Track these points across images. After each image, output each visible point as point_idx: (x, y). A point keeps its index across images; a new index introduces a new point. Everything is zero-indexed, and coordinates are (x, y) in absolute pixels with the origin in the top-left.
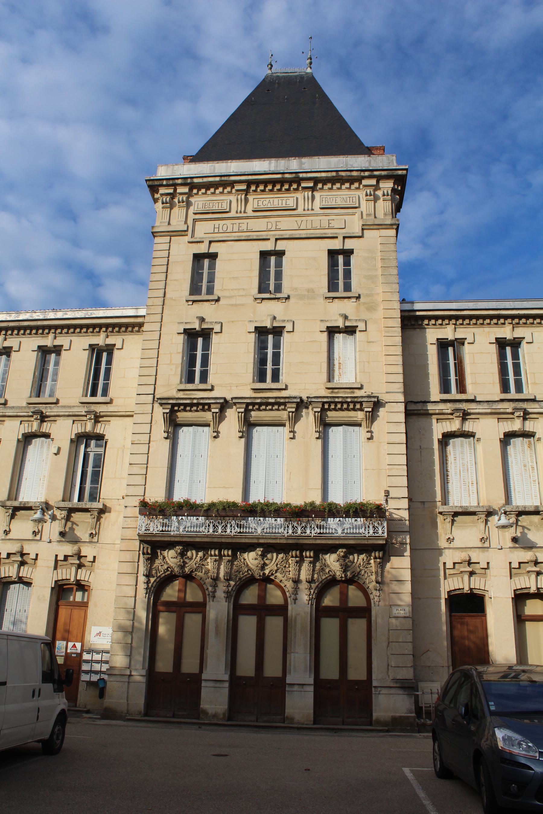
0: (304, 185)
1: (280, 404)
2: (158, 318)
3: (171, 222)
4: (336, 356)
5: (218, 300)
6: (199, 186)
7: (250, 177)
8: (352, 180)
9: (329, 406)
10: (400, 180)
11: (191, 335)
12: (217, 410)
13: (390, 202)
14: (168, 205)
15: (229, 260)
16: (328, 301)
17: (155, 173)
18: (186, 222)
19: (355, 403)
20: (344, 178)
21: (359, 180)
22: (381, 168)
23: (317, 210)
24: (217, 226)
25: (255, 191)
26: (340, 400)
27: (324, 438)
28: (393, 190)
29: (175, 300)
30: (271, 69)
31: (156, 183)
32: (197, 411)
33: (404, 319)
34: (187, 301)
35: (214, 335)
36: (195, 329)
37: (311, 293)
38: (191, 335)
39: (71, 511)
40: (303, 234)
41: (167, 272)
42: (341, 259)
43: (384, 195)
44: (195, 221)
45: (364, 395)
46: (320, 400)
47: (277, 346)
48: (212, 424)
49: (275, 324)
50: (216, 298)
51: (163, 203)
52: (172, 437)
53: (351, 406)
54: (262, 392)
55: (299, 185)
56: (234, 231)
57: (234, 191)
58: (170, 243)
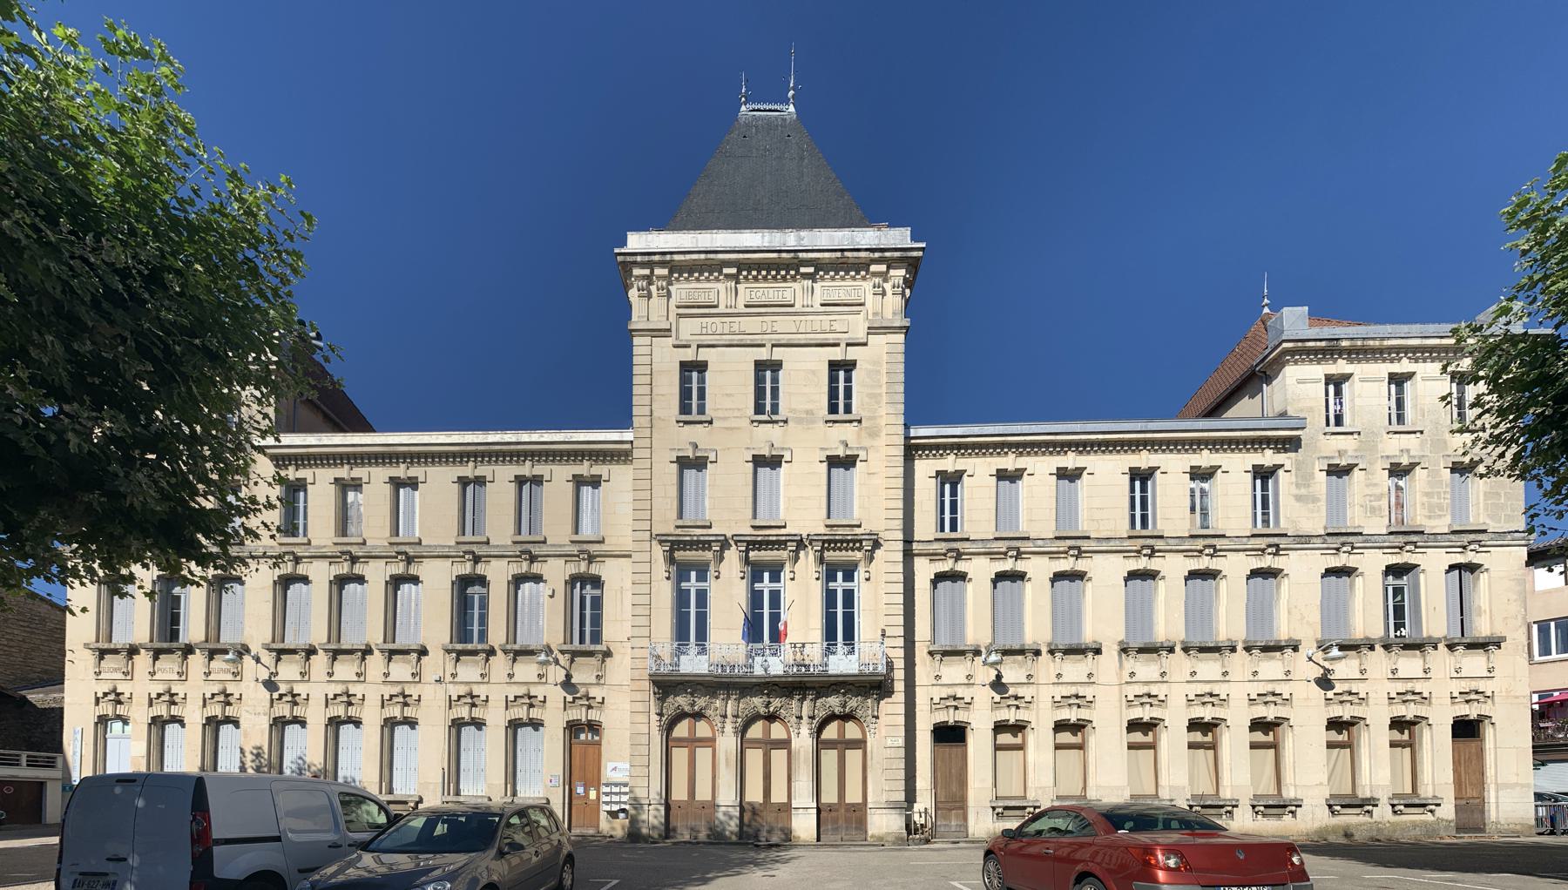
25: (746, 278)
37: (808, 418)
38: (684, 463)
39: (575, 654)
40: (801, 338)
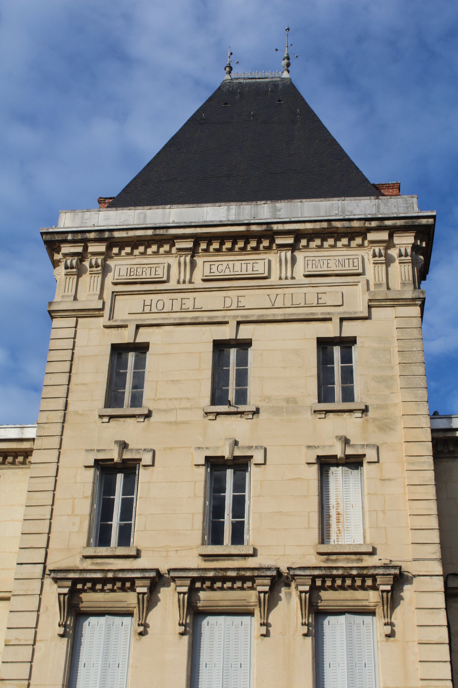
0: (279, 241)
1: (244, 579)
2: (55, 442)
3: (78, 297)
4: (332, 501)
5: (148, 415)
6: (122, 244)
7: (199, 230)
8: (351, 234)
9: (324, 582)
10: (425, 234)
11: (106, 470)
12: (145, 590)
13: (410, 265)
14: (75, 270)
15: (166, 354)
16: (319, 416)
17: (55, 222)
18: (101, 297)
19: (364, 577)
20: (340, 231)
21: (363, 233)
22: (395, 215)
23: (300, 278)
24: (148, 303)
25: (206, 250)
26: (340, 572)
27: (316, 634)
28: (415, 247)
29: (82, 415)
30: (229, 73)
31: (57, 237)
32: (112, 591)
33: (435, 442)
34: (101, 416)
35: (141, 469)
36: (113, 460)
37: (291, 405)
38: (106, 470)
40: (279, 314)
41: (70, 372)
42: (337, 352)
43: (400, 255)
44: (115, 294)
45: (379, 563)
46: (308, 572)
47: (240, 486)
48: (136, 611)
49: (237, 453)
50: (146, 412)
51: (66, 268)
52: (73, 636)
53: (358, 582)
54: (217, 560)
55: (272, 241)
56: (174, 310)
57: (174, 250)
58: (76, 327)
